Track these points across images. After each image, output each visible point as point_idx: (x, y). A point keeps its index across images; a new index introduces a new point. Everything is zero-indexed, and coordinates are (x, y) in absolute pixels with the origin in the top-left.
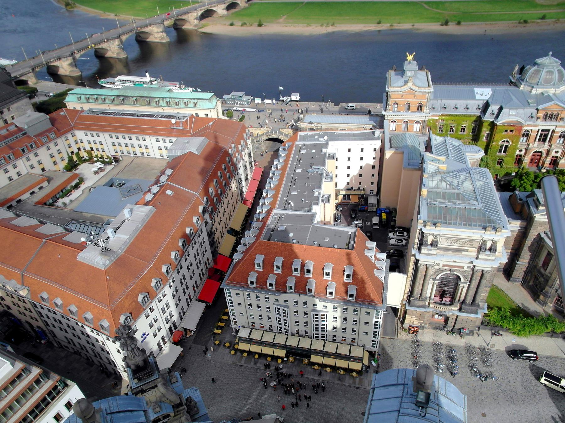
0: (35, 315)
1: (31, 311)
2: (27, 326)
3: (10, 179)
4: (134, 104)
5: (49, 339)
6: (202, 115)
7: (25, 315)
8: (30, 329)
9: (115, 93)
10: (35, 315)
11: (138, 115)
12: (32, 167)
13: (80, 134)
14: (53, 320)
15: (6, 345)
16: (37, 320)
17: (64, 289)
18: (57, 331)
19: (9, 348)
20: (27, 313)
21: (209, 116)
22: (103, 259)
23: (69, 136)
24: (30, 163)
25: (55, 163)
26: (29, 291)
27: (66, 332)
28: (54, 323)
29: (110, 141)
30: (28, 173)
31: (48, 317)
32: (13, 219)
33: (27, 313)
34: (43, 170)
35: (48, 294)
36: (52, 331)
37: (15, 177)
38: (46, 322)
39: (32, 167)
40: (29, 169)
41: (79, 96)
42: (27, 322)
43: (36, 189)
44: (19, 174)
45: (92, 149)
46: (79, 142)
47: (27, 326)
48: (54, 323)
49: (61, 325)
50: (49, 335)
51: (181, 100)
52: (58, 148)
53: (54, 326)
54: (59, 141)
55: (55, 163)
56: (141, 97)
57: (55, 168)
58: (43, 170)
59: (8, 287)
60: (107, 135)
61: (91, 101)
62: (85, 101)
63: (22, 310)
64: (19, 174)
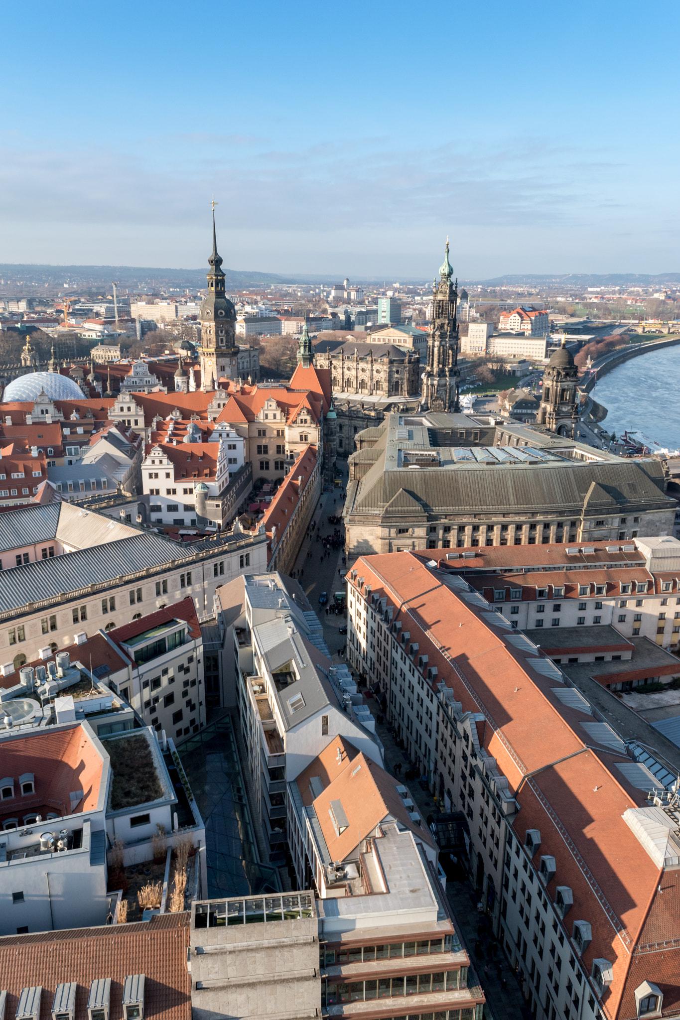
0: (499, 854)
1: (497, 844)
2: (475, 862)
3: (581, 621)
5: (492, 908)
7: (485, 843)
8: (475, 870)
10: (499, 854)
12: (622, 619)
14: (520, 886)
15: (443, 873)
16: (496, 865)
17: (573, 850)
18: (513, 909)
19: (443, 881)
20: (490, 843)
22: (670, 849)
25: (660, 630)
26: (517, 811)
27: (527, 923)
28: (519, 893)
30: (610, 626)
31: (516, 875)
32: (558, 685)
33: (490, 843)
34: (636, 631)
35: (542, 839)
36: (505, 904)
37: (589, 622)
38: (507, 880)
39: (622, 619)
40: (616, 619)
42: (479, 856)
43: (608, 657)
44: (597, 620)
47: (475, 862)
48: (519, 893)
49: (526, 905)
50: (497, 905)
53: (514, 897)
55: (660, 630)
57: (653, 637)
58: (636, 631)
59: (492, 783)
63: (487, 832)
64: (597, 620)
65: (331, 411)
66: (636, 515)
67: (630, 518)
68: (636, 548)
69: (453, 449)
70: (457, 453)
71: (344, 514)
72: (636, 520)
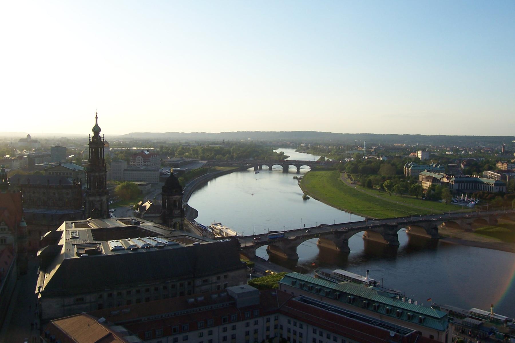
4: (350, 303)
6: (426, 334)
9: (333, 286)
11: (352, 316)
13: (283, 320)
21: (435, 338)
23: (272, 318)
24: (225, 334)
29: (311, 335)
41: (294, 280)
45: (289, 339)
46: (279, 327)
51: (406, 312)
52: (256, 327)
54: (260, 320)
56: (360, 297)
60: (311, 329)
61: (304, 288)
62: (298, 287)
65: (23, 221)
66: (225, 274)
67: (222, 276)
68: (228, 294)
69: (109, 242)
70: (113, 244)
71: (37, 291)
72: (226, 277)
